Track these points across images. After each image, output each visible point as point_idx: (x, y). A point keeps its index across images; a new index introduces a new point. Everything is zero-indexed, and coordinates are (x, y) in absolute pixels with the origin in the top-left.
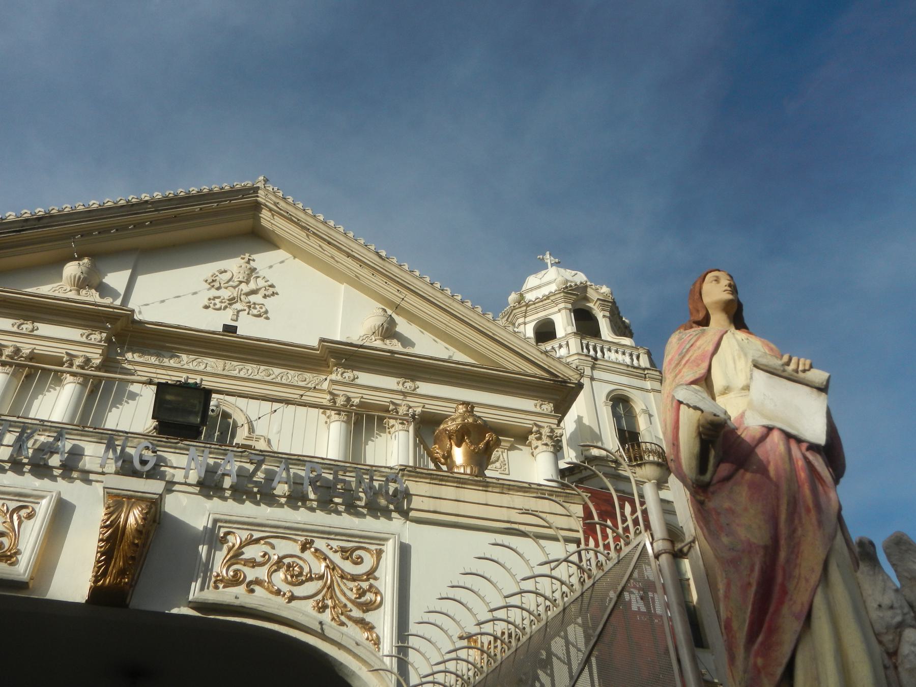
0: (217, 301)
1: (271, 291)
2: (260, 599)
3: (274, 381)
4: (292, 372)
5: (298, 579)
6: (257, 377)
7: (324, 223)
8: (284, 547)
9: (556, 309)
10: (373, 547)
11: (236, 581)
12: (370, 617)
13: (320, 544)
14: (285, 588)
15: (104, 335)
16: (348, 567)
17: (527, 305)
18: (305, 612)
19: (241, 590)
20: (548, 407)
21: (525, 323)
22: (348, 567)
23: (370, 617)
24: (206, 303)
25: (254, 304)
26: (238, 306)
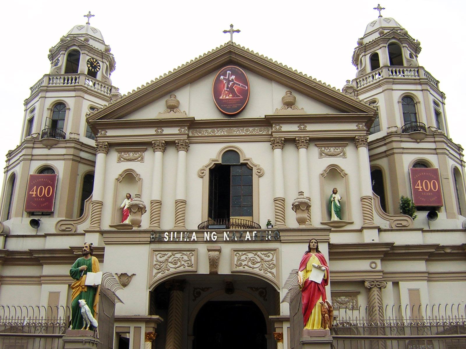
2: (247, 269)
3: (250, 134)
4: (256, 128)
6: (243, 134)
9: (378, 47)
10: (272, 252)
11: (241, 265)
12: (272, 271)
13: (259, 253)
14: (252, 266)
15: (186, 128)
16: (266, 259)
17: (365, 46)
18: (257, 271)
19: (241, 267)
20: (362, 126)
21: (365, 55)
22: (266, 259)
23: (272, 271)
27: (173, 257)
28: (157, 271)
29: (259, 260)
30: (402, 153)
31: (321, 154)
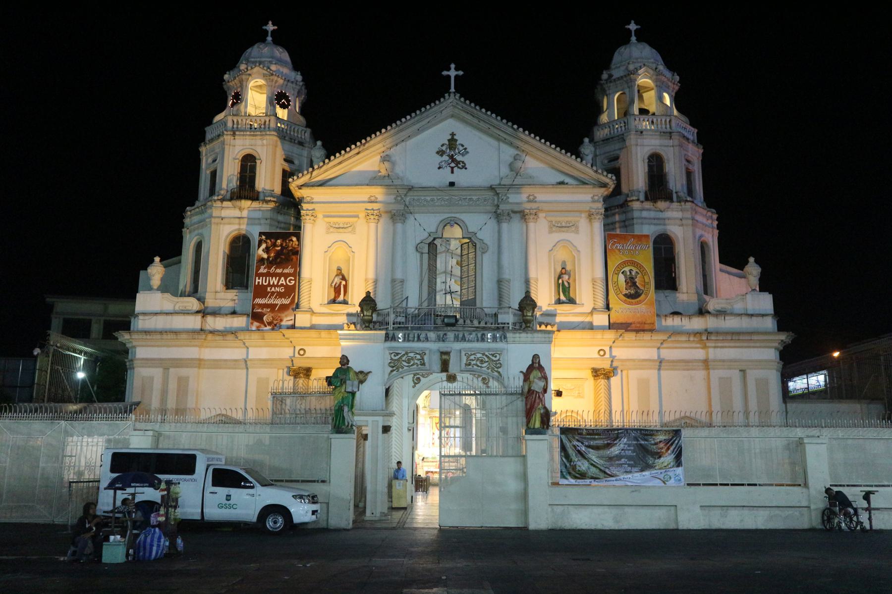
0: (443, 163)
1: (466, 151)
5: (482, 362)
6: (466, 204)
7: (486, 114)
8: (479, 355)
11: (470, 364)
12: (499, 370)
14: (480, 365)
16: (494, 359)
19: (470, 367)
22: (494, 359)
23: (499, 370)
24: (438, 166)
25: (461, 161)
26: (453, 165)
27: (406, 356)
28: (391, 369)
29: (487, 360)
30: (642, 224)
31: (551, 228)
